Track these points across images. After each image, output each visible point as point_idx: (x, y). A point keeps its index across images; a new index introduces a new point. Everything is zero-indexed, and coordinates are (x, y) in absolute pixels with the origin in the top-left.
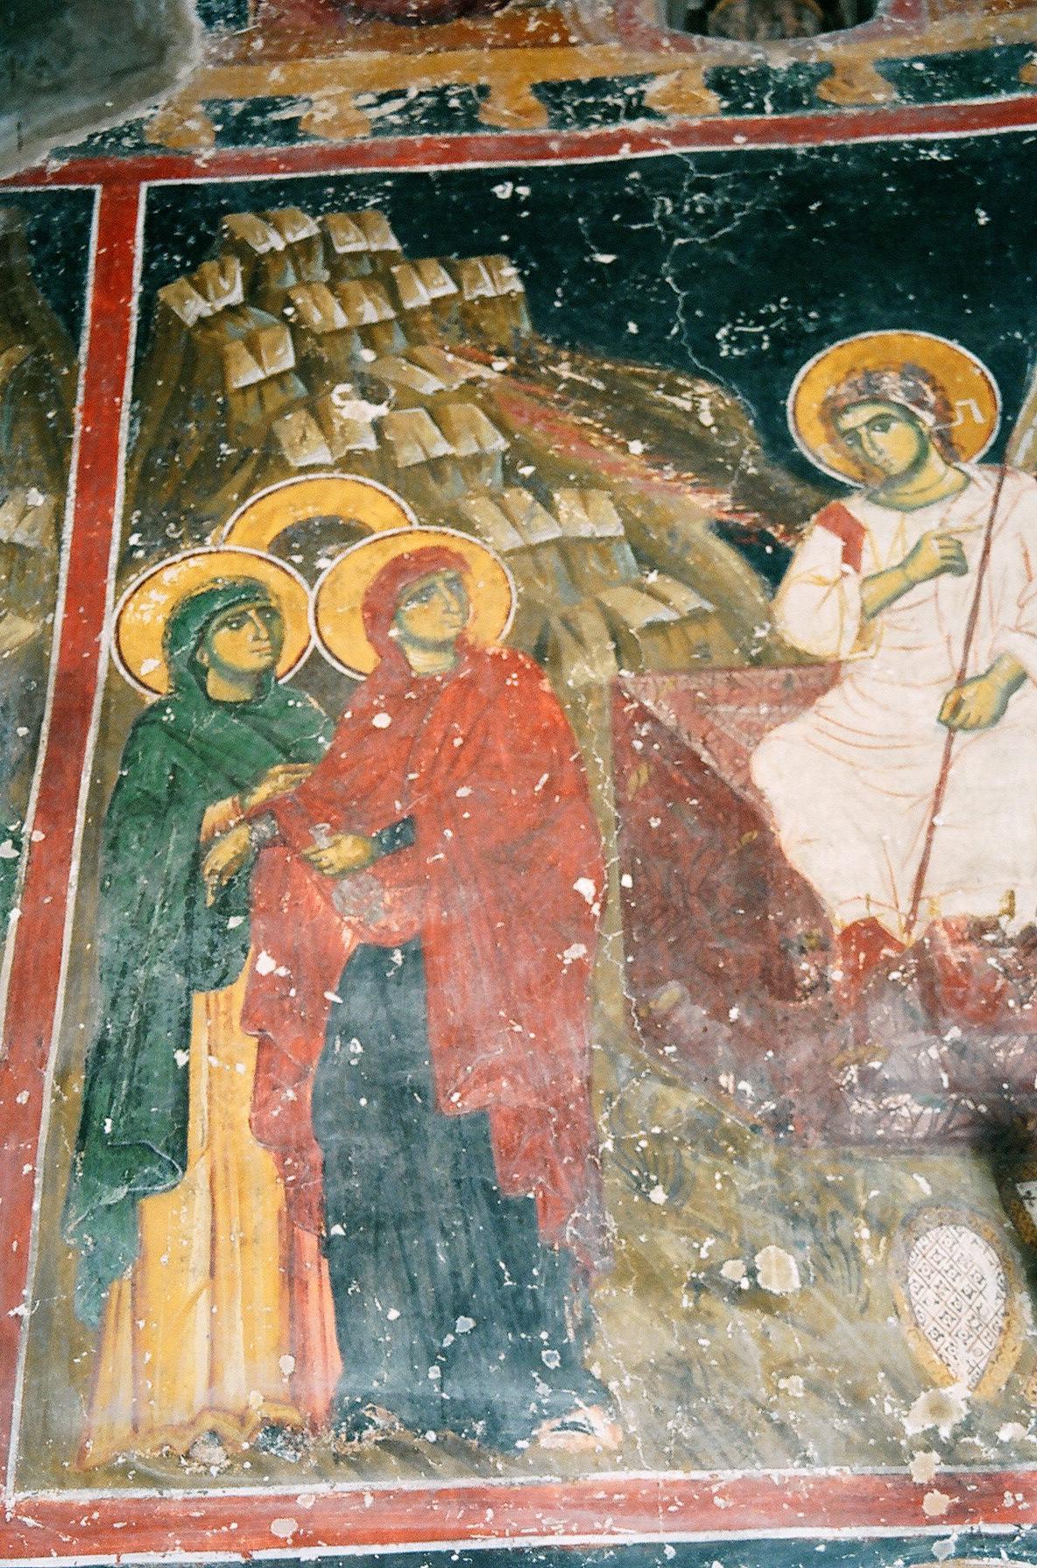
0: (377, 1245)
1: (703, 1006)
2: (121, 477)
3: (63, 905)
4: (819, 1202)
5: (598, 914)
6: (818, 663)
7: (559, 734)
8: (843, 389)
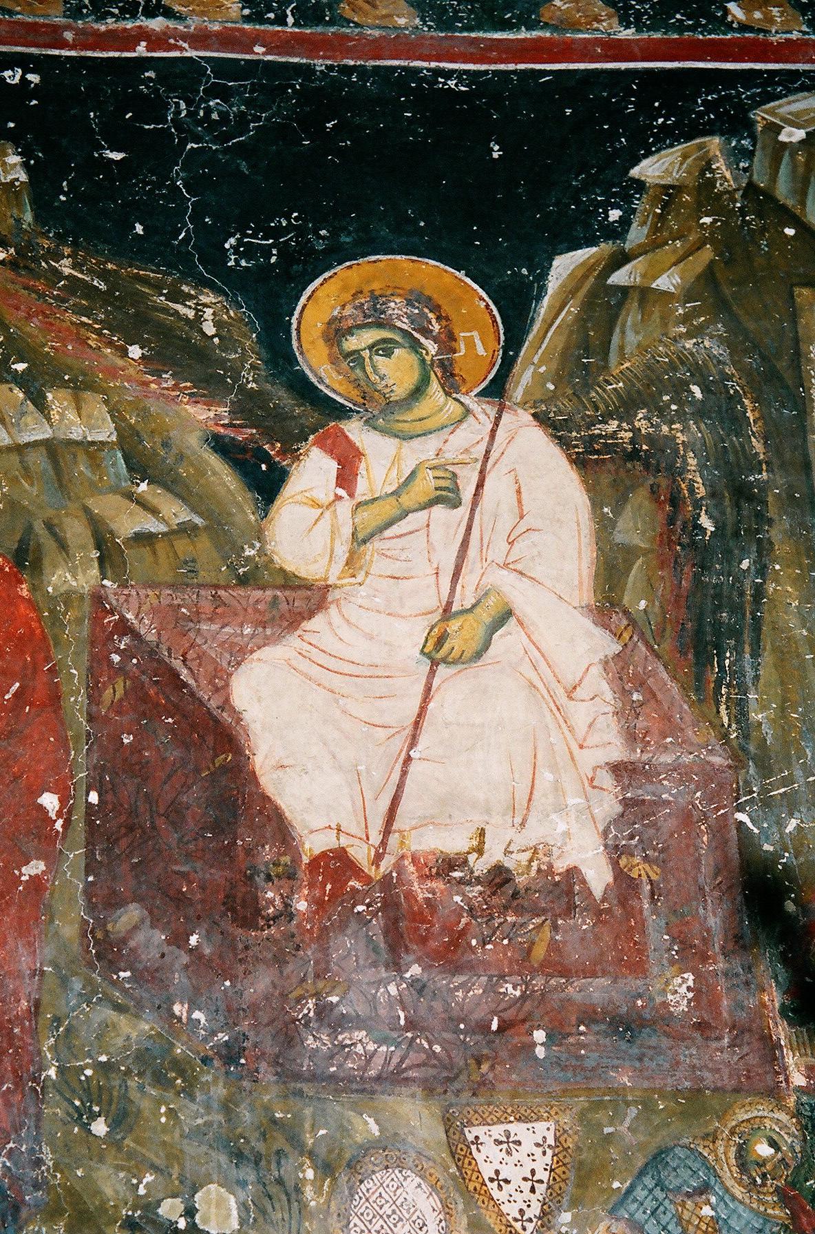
1: (163, 931)
4: (265, 1140)
6: (309, 587)
7: (35, 644)
8: (348, 311)
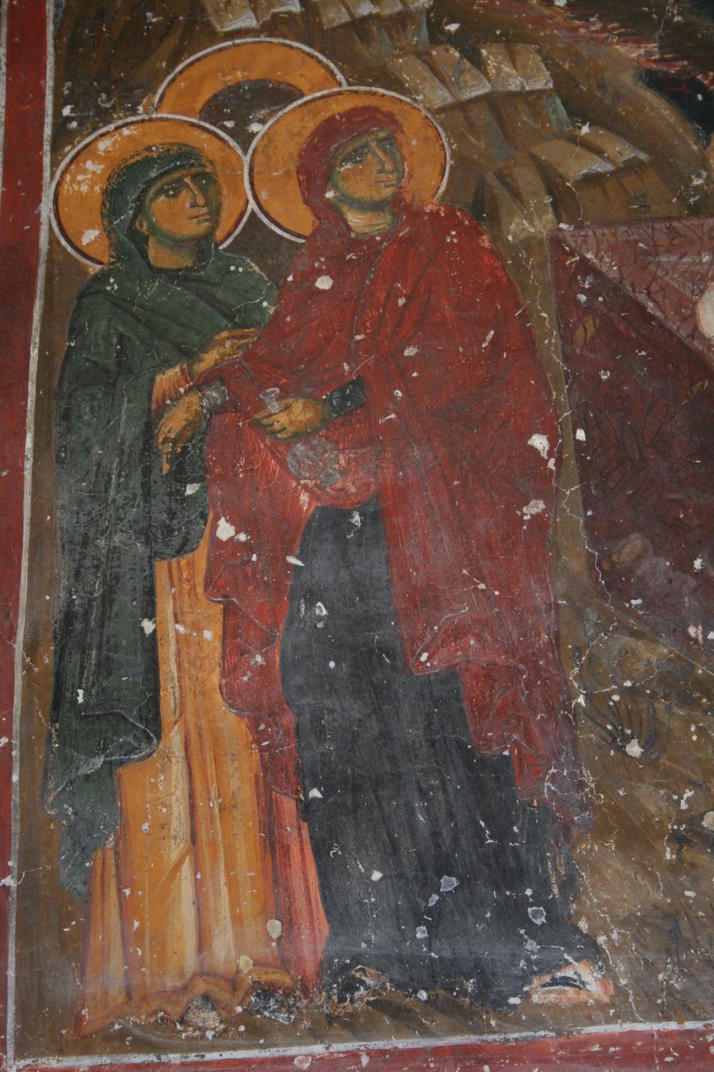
0: (356, 806)
1: (667, 559)
2: (50, 49)
3: (22, 478)
5: (554, 468)
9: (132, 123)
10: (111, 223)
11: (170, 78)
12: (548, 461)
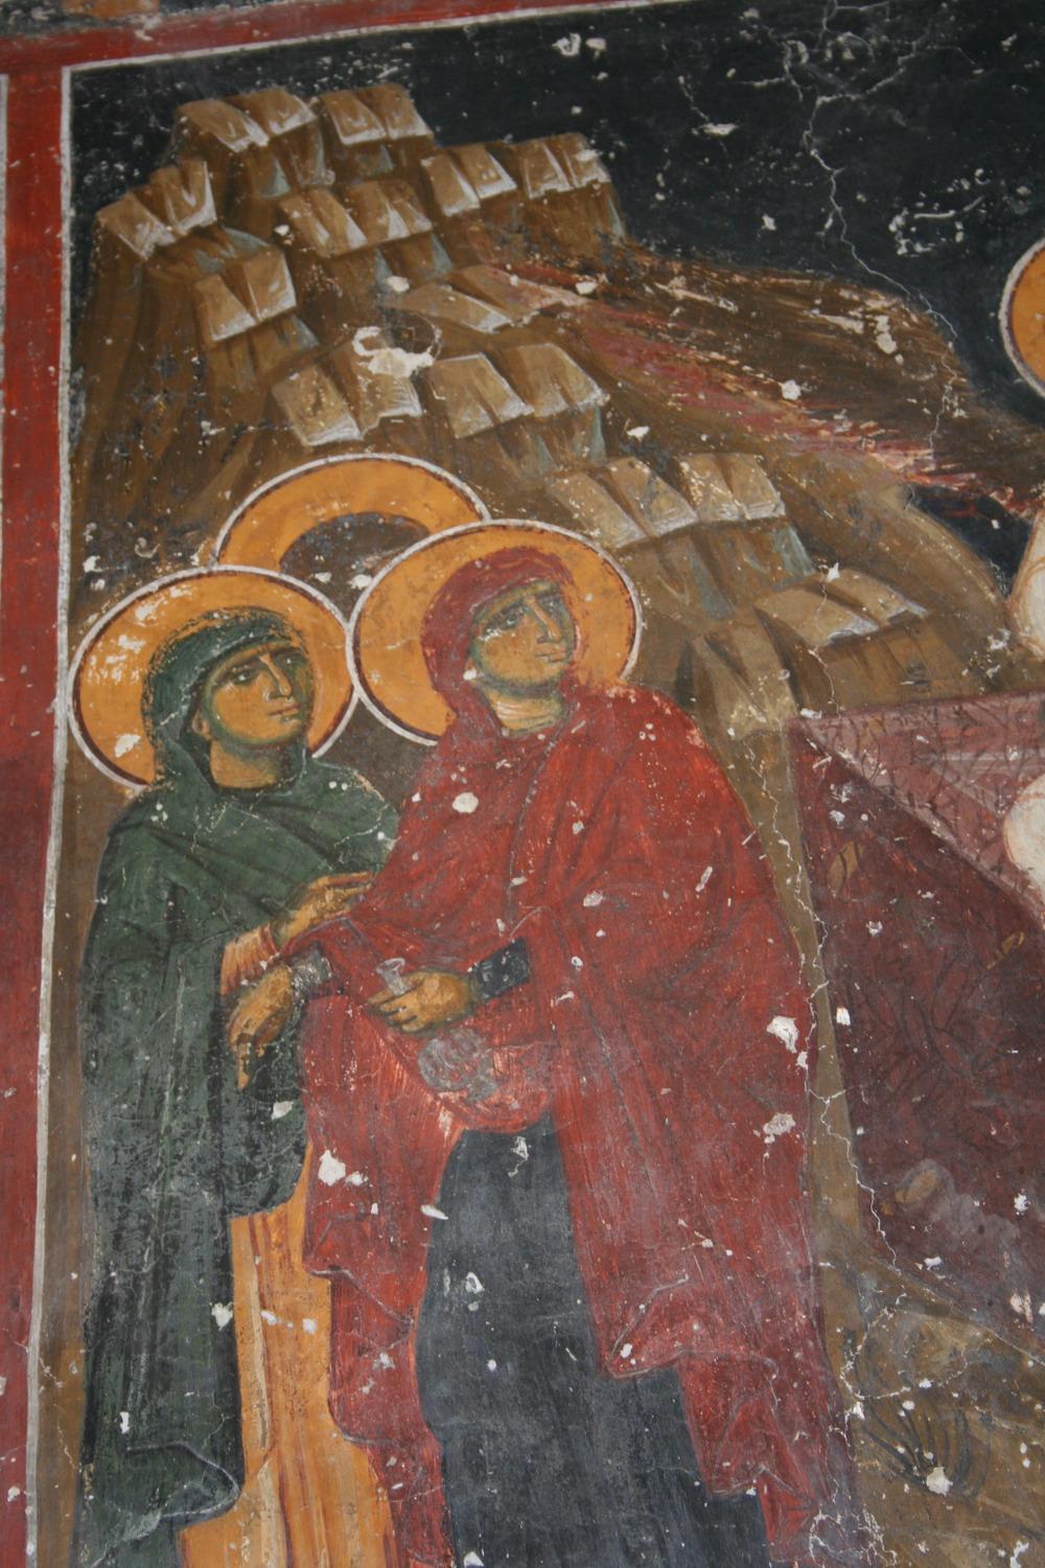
1: (974, 1196)
3: (33, 1099)
5: (806, 1067)
9: (184, 580)
10: (156, 724)
11: (236, 513)
12: (796, 1055)
